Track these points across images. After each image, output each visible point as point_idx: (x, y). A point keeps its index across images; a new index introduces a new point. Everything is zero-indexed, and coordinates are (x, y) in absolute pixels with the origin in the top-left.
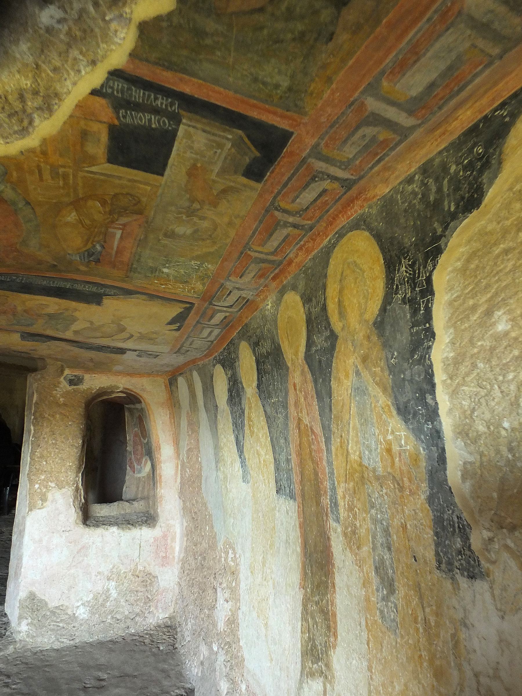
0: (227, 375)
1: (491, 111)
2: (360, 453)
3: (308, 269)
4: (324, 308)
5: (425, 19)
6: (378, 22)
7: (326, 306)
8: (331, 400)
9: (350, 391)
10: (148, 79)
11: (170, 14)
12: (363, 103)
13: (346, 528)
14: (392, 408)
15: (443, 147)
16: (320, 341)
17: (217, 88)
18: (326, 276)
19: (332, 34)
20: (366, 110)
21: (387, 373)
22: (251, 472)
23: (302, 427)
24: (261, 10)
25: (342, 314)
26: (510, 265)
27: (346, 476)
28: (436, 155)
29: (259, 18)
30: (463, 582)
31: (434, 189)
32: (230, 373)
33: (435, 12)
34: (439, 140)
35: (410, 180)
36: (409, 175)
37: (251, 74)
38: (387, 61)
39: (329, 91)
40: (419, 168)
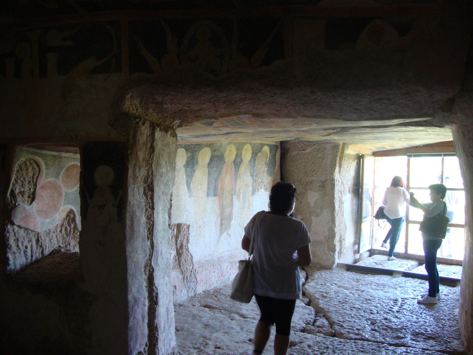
0: (187, 154)
4: (241, 154)
16: (238, 160)
32: (190, 155)
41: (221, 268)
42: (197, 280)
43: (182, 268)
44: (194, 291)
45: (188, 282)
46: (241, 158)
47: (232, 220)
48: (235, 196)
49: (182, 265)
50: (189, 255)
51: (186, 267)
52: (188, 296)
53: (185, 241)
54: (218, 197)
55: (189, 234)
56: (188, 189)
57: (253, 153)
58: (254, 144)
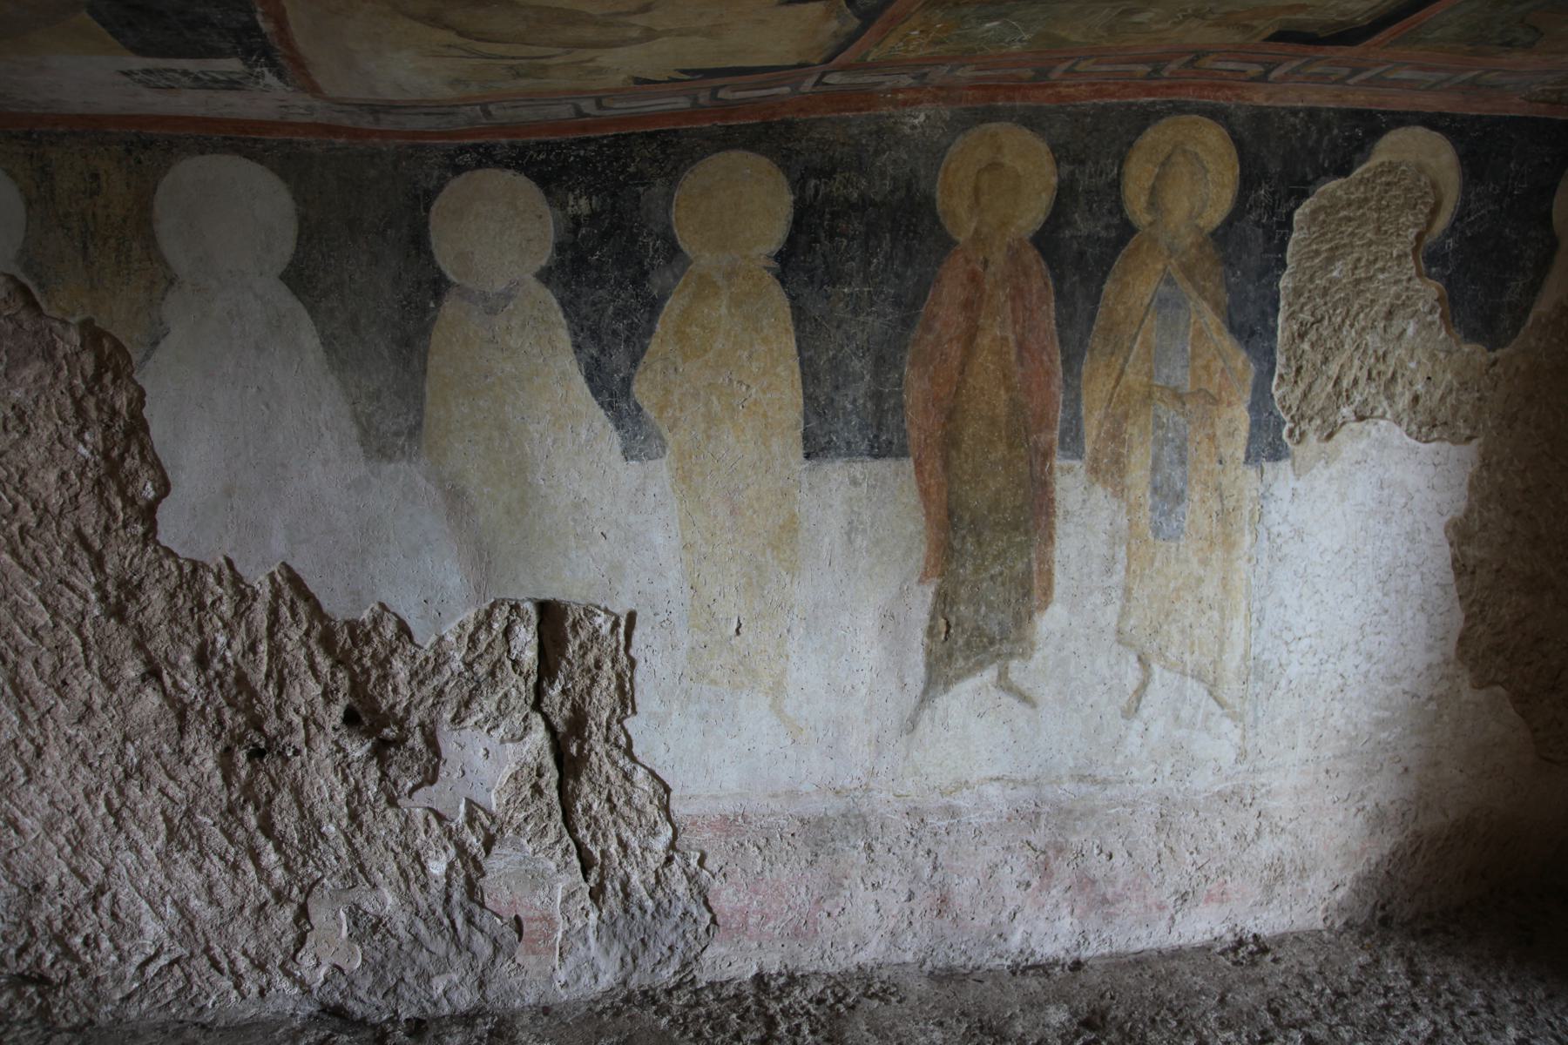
2: (1150, 370)
3: (1085, 115)
4: (1116, 185)
7: (1119, 184)
8: (1096, 309)
9: (1147, 301)
13: (1096, 460)
14: (1223, 325)
15: (1331, 106)
16: (1083, 225)
18: (1130, 144)
21: (1222, 290)
22: (667, 436)
23: (984, 341)
25: (1153, 204)
26: (1350, 229)
27: (1110, 400)
30: (1267, 466)
31: (1315, 136)
35: (1294, 112)
41: (935, 868)
42: (710, 910)
43: (582, 832)
44: (685, 965)
45: (635, 910)
46: (1118, 207)
47: (1044, 606)
48: (1077, 464)
49: (581, 822)
50: (640, 774)
51: (618, 836)
52: (625, 983)
53: (603, 699)
54: (909, 464)
55: (632, 663)
56: (608, 406)
57: (1248, 182)
58: (1261, 116)
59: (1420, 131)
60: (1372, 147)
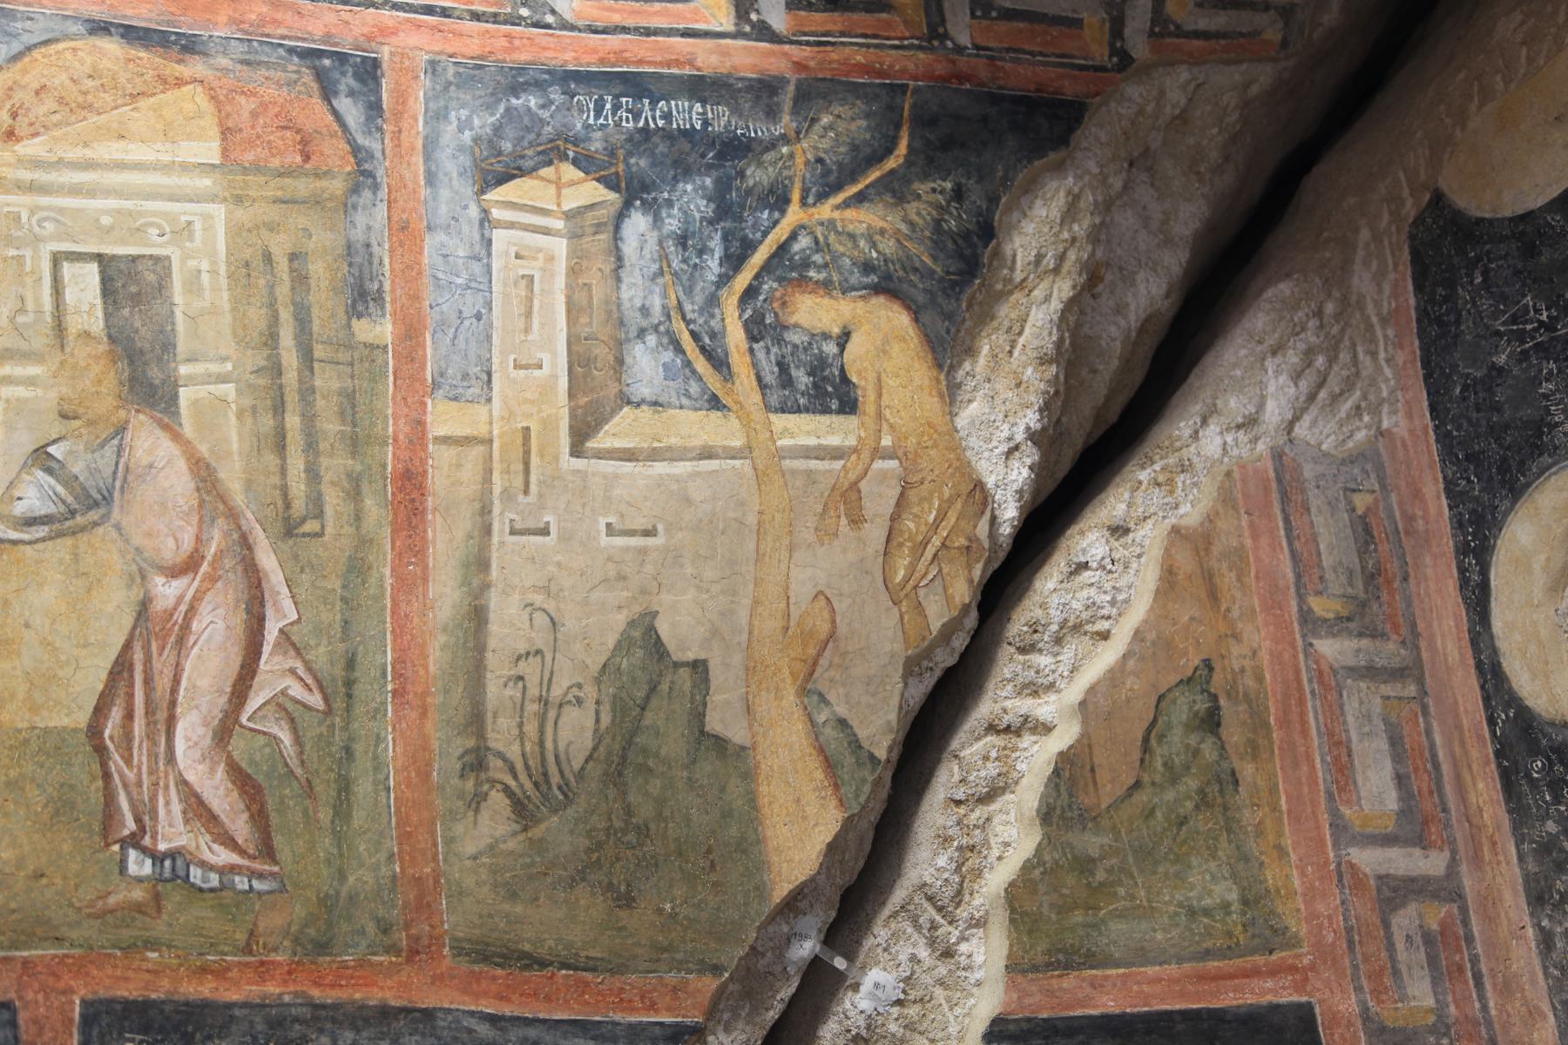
1: (1493, 743)
5: (1309, 696)
6: (1266, 725)
10: (1045, 1016)
11: (1039, 850)
12: (1350, 862)
15: (1513, 850)
17: (1152, 971)
19: (1233, 773)
20: (1366, 875)
24: (1138, 785)
28: (1521, 868)
29: (1141, 797)
33: (1310, 681)
34: (1501, 858)
36: (1538, 947)
37: (1180, 905)
38: (1320, 774)
39: (1295, 872)
40: (1532, 915)
59: (1497, 625)
60: (1552, 724)
